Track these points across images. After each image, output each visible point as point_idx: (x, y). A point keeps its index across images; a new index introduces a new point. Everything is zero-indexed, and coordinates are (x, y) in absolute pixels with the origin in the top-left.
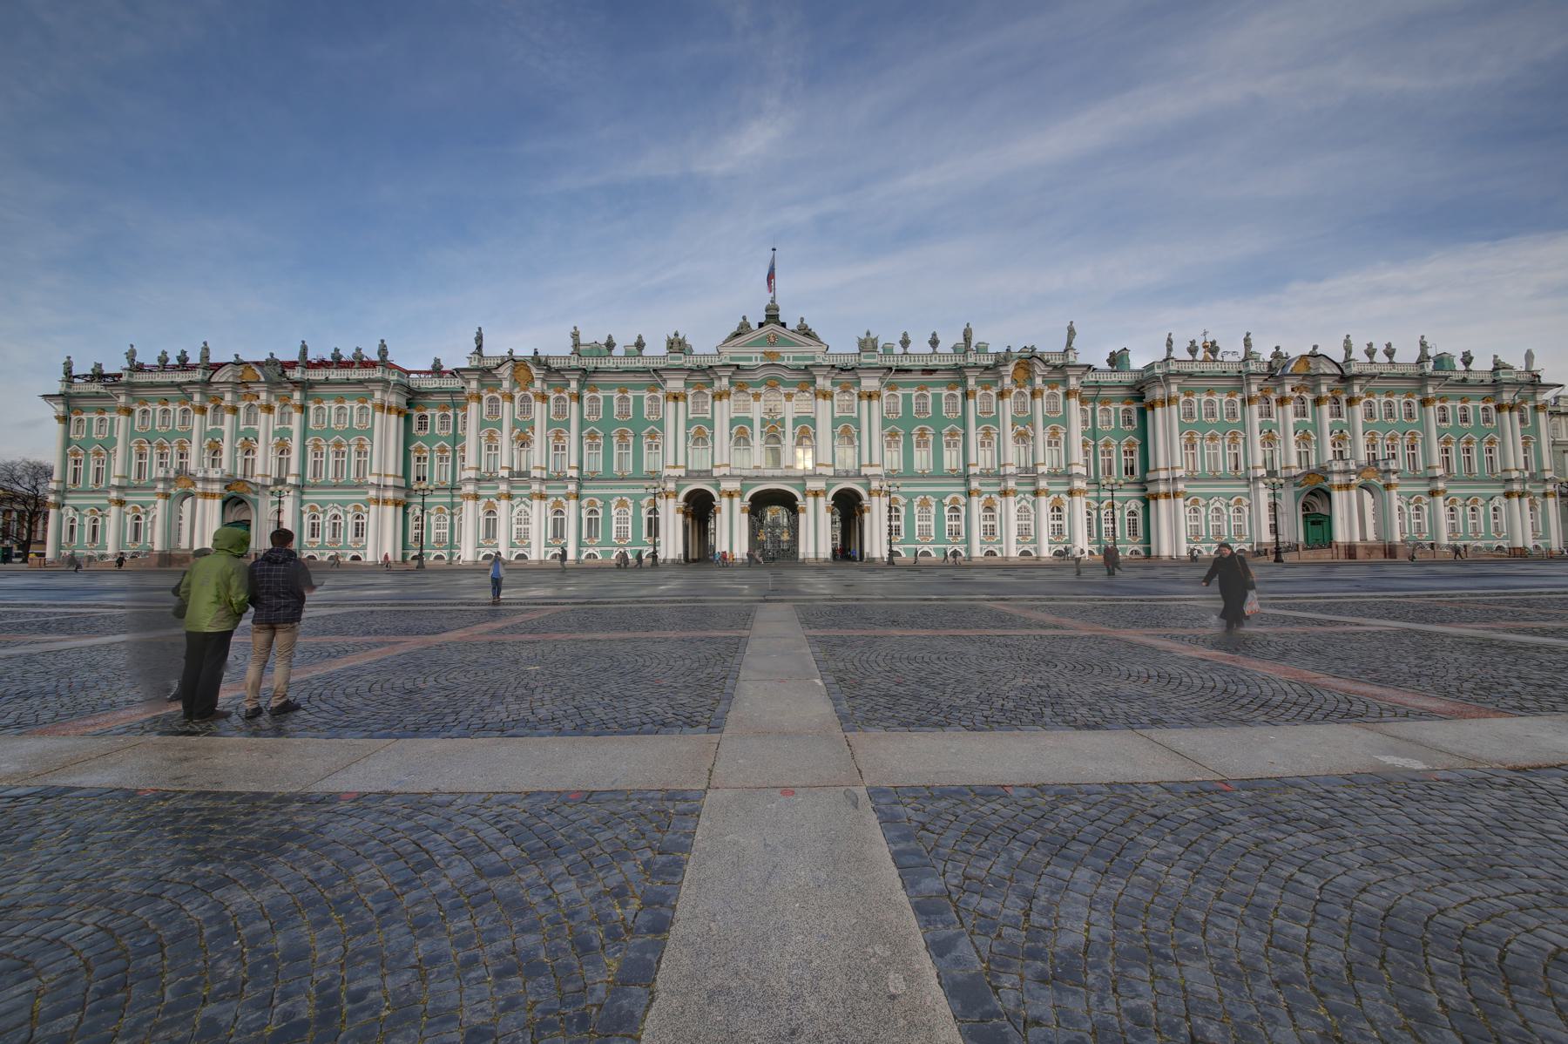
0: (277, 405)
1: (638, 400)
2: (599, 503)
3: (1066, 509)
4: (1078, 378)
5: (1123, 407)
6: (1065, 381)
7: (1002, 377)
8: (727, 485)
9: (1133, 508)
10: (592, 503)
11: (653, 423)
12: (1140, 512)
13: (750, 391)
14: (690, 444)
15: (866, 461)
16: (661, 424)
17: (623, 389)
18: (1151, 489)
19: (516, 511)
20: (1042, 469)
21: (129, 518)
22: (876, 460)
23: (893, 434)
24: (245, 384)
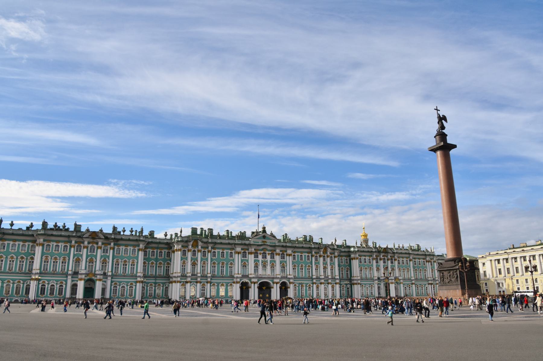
0: (103, 246)
1: (227, 253)
2: (216, 284)
6: (334, 253)
8: (253, 280)
11: (232, 260)
13: (259, 252)
15: (288, 274)
16: (233, 260)
17: (223, 249)
18: (353, 282)
20: (330, 277)
21: (40, 285)
23: (295, 266)
24: (93, 238)
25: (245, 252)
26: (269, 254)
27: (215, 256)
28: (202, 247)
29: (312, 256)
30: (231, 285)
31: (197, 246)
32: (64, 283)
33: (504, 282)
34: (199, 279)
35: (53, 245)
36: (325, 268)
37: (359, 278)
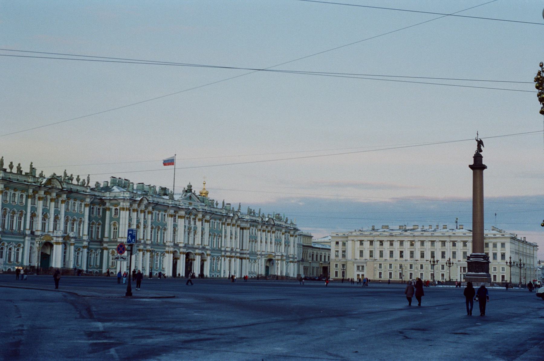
13: (187, 216)
15: (205, 244)
20: (234, 250)
23: (210, 235)
25: (175, 216)
26: (193, 219)
30: (164, 255)
32: (22, 245)
33: (365, 265)
35: (11, 193)
36: (231, 238)
37: (248, 252)
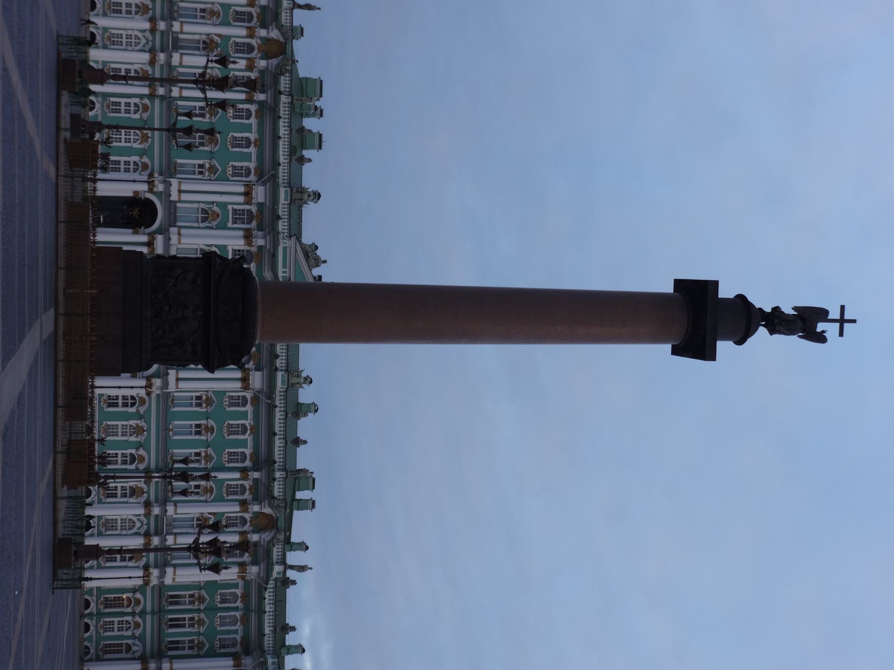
3: (131, 564)
4: (259, 574)
5: (238, 637)
6: (254, 563)
7: (260, 504)
9: (134, 648)
10: (146, 108)
11: (224, 171)
12: (129, 656)
14: (202, 206)
15: (183, 374)
16: (223, 179)
17: (259, 143)
19: (140, 35)
22: (183, 385)
23: (209, 402)
27: (235, 117)
28: (262, 72)
29: (244, 471)
31: (267, 56)
34: (162, 57)
